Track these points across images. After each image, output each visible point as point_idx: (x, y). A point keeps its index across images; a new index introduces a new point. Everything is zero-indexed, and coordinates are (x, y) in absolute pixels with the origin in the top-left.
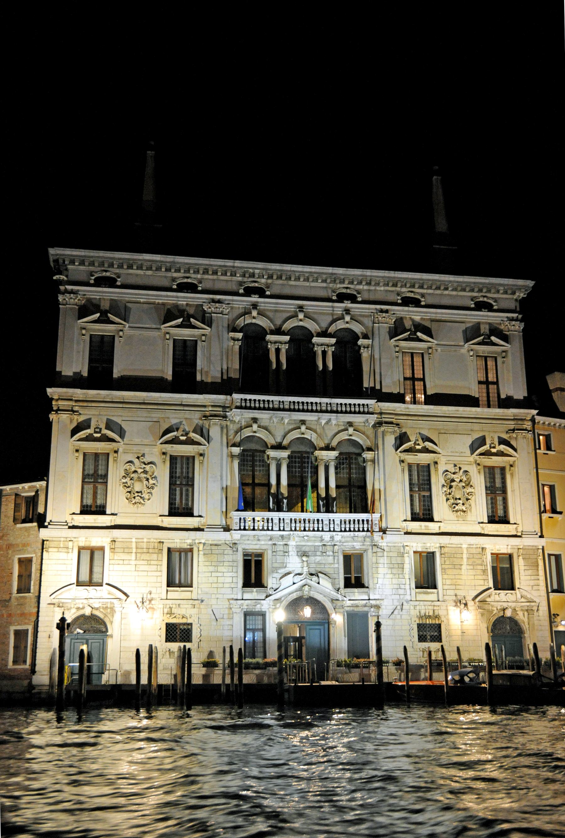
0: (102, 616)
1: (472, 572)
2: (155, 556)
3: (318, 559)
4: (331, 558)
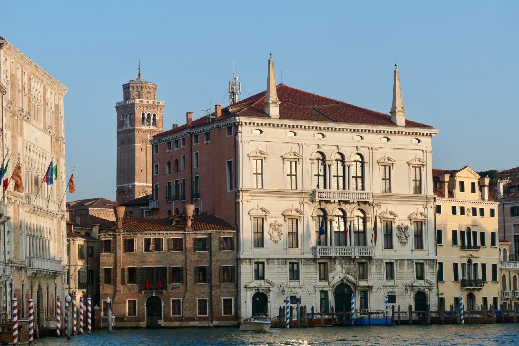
0: (265, 293)
1: (408, 272)
2: (284, 266)
3: (348, 266)
4: (353, 266)
